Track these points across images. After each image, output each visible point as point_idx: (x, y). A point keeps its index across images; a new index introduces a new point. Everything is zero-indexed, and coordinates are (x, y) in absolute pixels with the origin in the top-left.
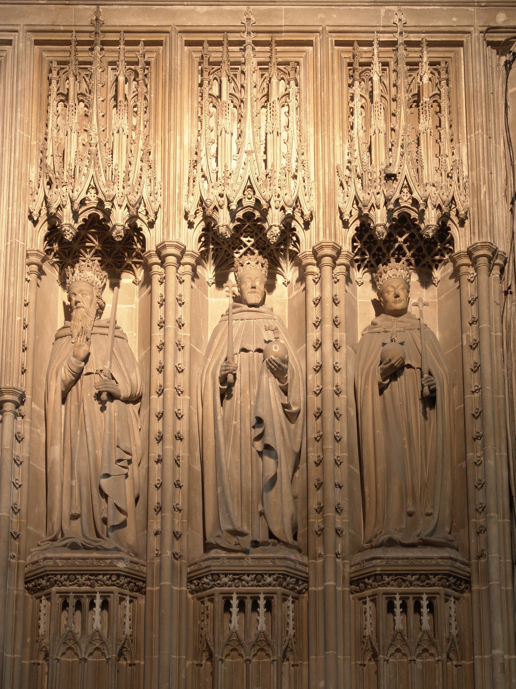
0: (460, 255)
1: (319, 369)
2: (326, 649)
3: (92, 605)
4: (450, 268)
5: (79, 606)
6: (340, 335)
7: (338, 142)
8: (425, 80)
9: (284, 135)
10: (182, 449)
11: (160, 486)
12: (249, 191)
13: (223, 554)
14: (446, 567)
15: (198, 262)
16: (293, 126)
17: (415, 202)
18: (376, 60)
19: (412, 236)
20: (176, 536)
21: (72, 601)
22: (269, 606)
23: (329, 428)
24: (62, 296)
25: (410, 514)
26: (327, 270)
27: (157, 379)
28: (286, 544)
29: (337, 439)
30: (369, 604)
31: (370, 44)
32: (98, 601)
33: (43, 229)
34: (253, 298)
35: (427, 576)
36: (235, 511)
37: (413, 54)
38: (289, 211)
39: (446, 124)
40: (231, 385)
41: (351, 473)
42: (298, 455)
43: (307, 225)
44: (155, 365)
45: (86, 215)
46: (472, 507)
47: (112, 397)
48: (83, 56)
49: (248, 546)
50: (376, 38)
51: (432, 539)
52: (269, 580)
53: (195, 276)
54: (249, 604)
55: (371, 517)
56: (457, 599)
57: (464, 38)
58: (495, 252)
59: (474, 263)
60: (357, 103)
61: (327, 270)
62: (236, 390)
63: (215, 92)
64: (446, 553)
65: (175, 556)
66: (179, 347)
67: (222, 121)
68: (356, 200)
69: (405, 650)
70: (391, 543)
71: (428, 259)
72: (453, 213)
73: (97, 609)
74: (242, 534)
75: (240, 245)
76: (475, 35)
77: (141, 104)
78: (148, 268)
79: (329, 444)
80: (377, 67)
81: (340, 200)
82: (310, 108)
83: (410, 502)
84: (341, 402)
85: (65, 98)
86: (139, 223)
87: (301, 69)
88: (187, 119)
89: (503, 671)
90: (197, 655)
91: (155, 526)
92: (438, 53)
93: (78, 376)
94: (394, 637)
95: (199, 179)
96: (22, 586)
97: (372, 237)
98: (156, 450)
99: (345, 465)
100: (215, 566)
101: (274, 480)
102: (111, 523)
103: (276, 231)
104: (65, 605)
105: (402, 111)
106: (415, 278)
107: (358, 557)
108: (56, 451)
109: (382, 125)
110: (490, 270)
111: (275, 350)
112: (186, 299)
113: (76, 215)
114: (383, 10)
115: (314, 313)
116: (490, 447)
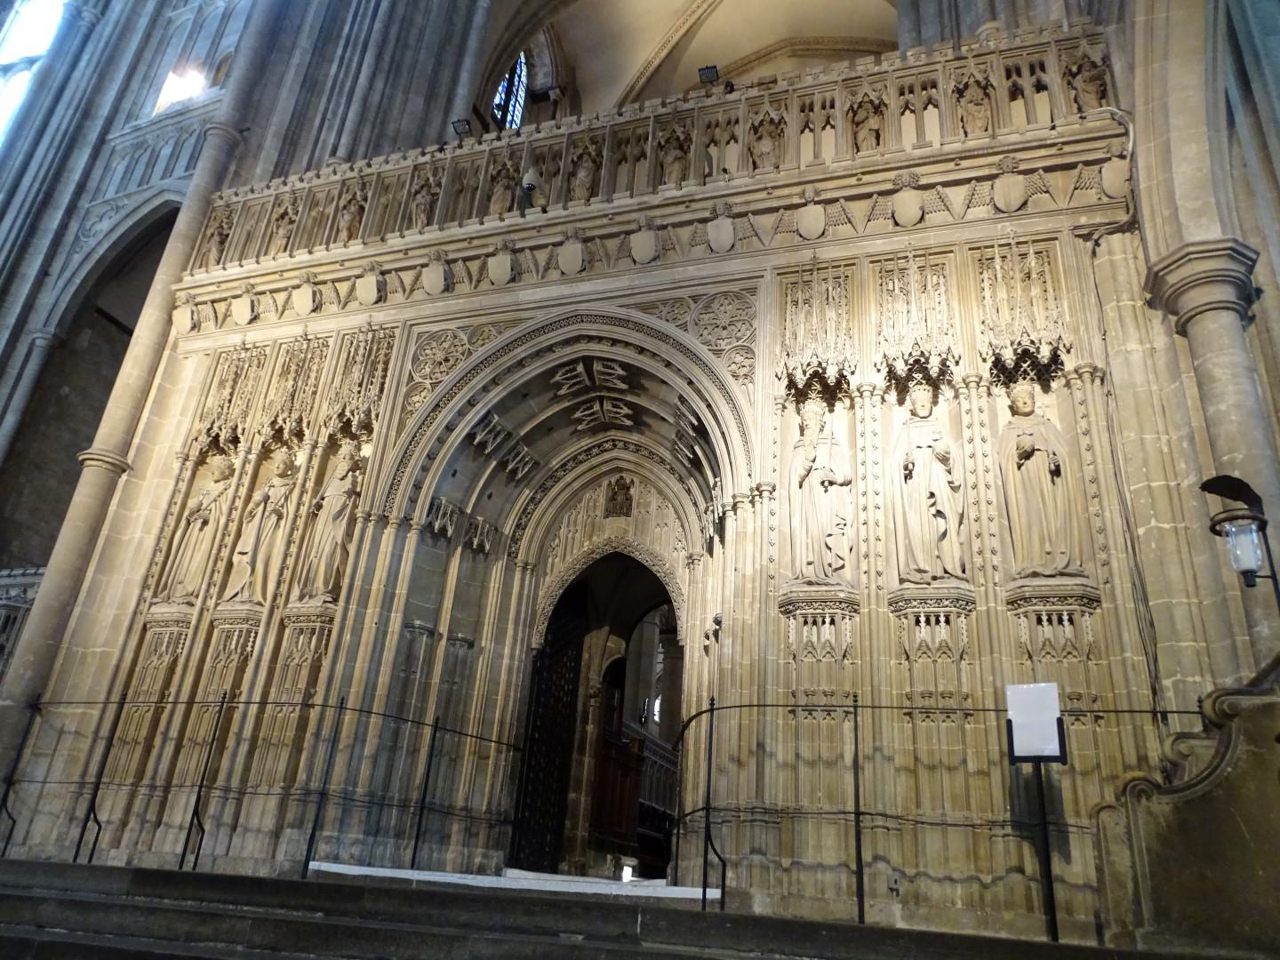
0: (1069, 373)
1: (973, 456)
2: (992, 652)
3: (824, 622)
4: (1063, 381)
5: (815, 623)
6: (986, 432)
7: (975, 309)
8: (1033, 264)
9: (938, 308)
10: (880, 515)
11: (866, 540)
12: (916, 347)
13: (913, 586)
14: (1079, 591)
15: (885, 392)
16: (944, 303)
17: (1032, 342)
18: (997, 256)
19: (1033, 363)
20: (879, 574)
21: (810, 620)
22: (947, 622)
23: (982, 495)
24: (798, 420)
25: (1049, 553)
26: (973, 391)
27: (861, 470)
28: (957, 577)
29: (989, 503)
30: (1023, 618)
31: (992, 247)
32: (828, 620)
33: (785, 382)
34: (923, 413)
35: (1065, 598)
36: (920, 556)
37: (1023, 249)
38: (944, 356)
39: (1050, 289)
40: (911, 472)
41: (1001, 525)
42: (962, 515)
43: (957, 363)
44: (859, 461)
45: (811, 372)
46: (1096, 547)
47: (831, 483)
48: (806, 279)
49: (929, 580)
50: (996, 243)
51: (1067, 571)
52: (946, 603)
53: (883, 400)
54: (933, 620)
55: (1019, 556)
56: (1091, 614)
57: (1058, 235)
58: (1095, 369)
59: (1080, 376)
60: (986, 284)
61: (973, 391)
62: (914, 473)
63: (891, 287)
64: (1078, 581)
65: (879, 588)
66: (875, 448)
67: (896, 305)
68: (991, 344)
69: (1053, 653)
70: (1035, 575)
71: (1046, 376)
72: (1061, 347)
73: (827, 625)
74: (925, 572)
75: (912, 379)
76: (1066, 232)
77: (844, 301)
78: (852, 399)
79: (983, 506)
80: (998, 261)
81: (979, 347)
82: (954, 291)
83: (1047, 544)
84: (990, 478)
85: (796, 303)
86: (845, 373)
87: (947, 267)
88: (873, 306)
89: (1134, 669)
90: (898, 656)
91: (864, 568)
92: (1040, 246)
93: (809, 471)
94: (1044, 645)
95: (883, 342)
96: (777, 610)
97: (1004, 366)
98: (862, 516)
99: (996, 521)
100: (907, 595)
101: (944, 534)
102: (834, 567)
103: (937, 370)
104: (806, 623)
105: (1019, 286)
106: (1037, 388)
107: (1012, 585)
108: (796, 521)
109: (1005, 296)
110: (1093, 381)
111: (940, 448)
112: (878, 417)
113: (804, 373)
114: (999, 226)
115: (966, 419)
116: (1105, 503)
